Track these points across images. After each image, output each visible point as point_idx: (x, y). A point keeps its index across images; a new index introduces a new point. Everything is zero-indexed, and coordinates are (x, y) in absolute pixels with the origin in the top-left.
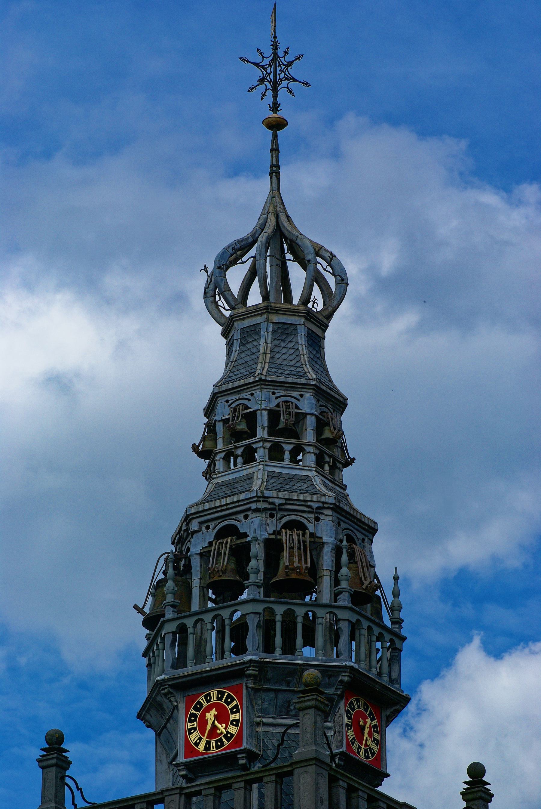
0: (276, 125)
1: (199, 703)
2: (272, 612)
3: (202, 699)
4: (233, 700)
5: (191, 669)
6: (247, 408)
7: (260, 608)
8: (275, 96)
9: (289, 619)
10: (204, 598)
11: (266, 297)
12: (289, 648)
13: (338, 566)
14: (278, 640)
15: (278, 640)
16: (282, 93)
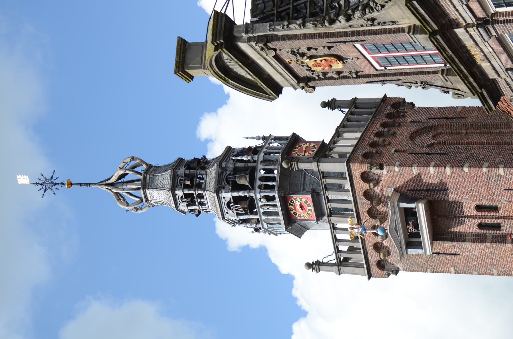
0: (71, 184)
1: (294, 213)
2: (260, 187)
3: (292, 212)
4: (292, 200)
5: (281, 217)
6: (182, 197)
7: (258, 190)
8: (58, 184)
9: (262, 179)
10: (256, 214)
11: (139, 189)
12: (273, 179)
13: (242, 161)
14: (270, 183)
15: (270, 183)
16: (57, 181)
